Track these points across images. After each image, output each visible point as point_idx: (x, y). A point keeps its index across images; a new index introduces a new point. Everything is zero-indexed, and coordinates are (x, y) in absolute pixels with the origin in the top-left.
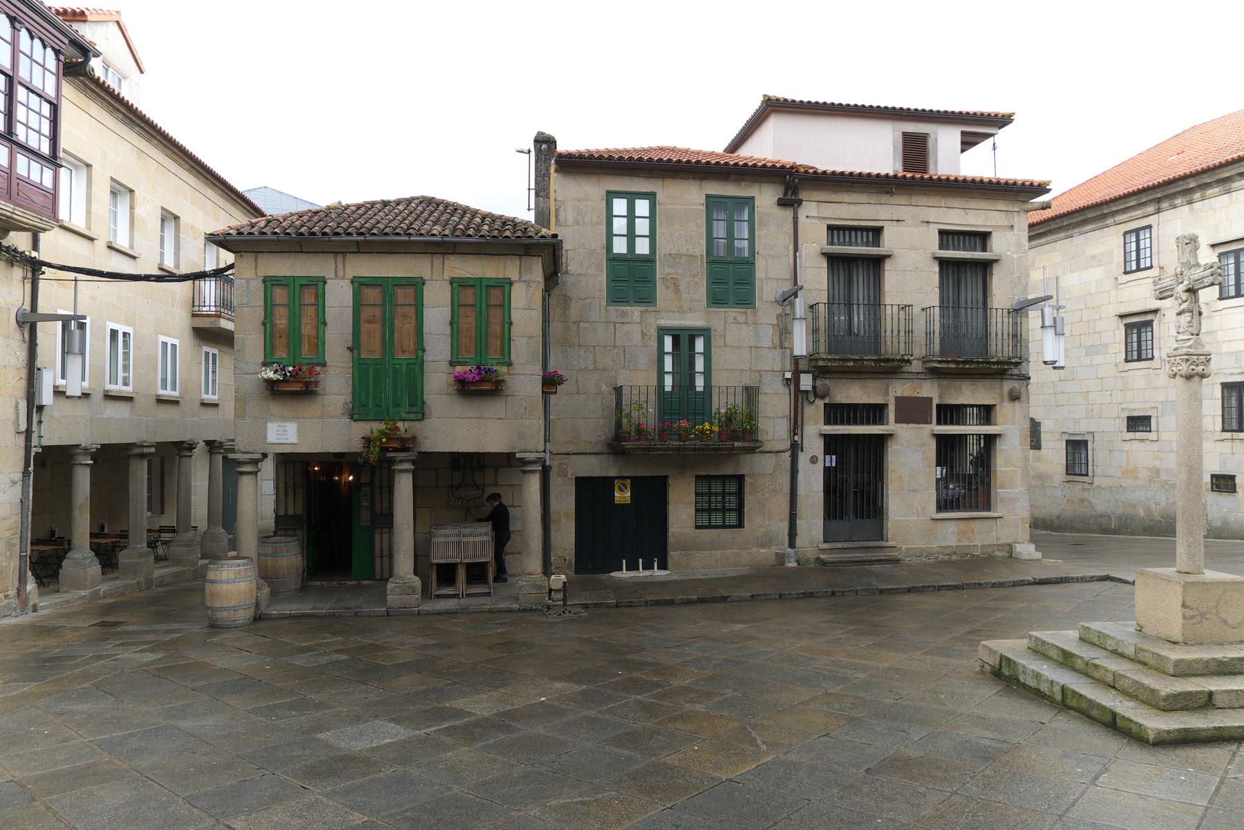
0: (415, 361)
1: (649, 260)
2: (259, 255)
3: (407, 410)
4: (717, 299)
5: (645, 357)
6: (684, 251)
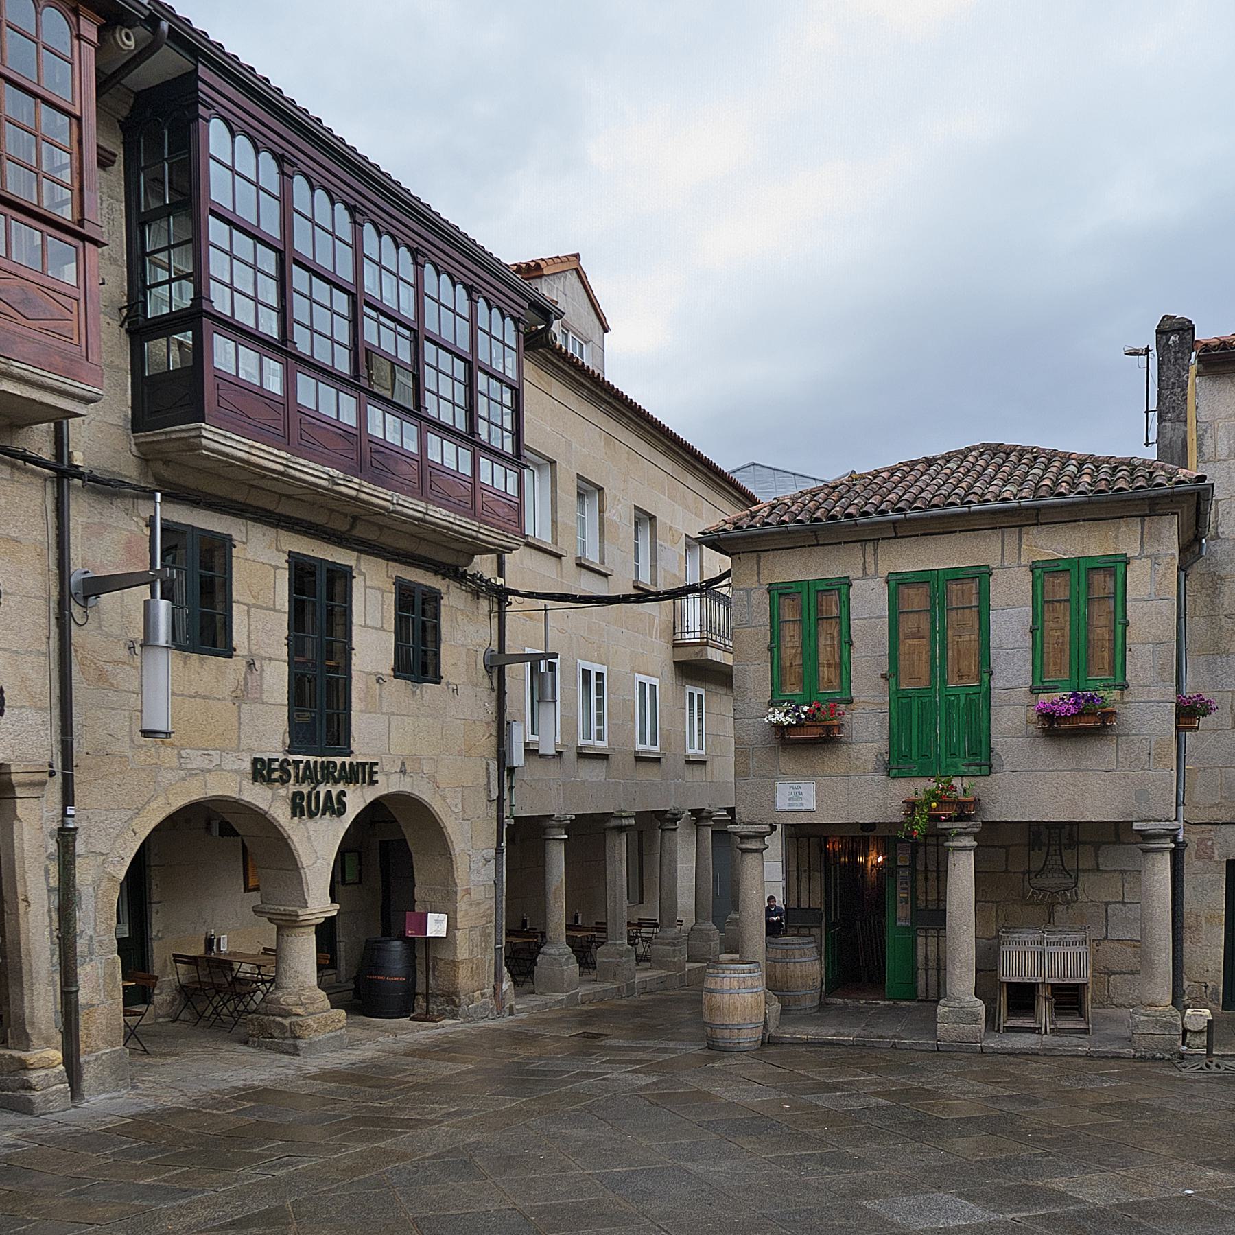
0: (976, 690)
2: (762, 555)
3: (966, 762)
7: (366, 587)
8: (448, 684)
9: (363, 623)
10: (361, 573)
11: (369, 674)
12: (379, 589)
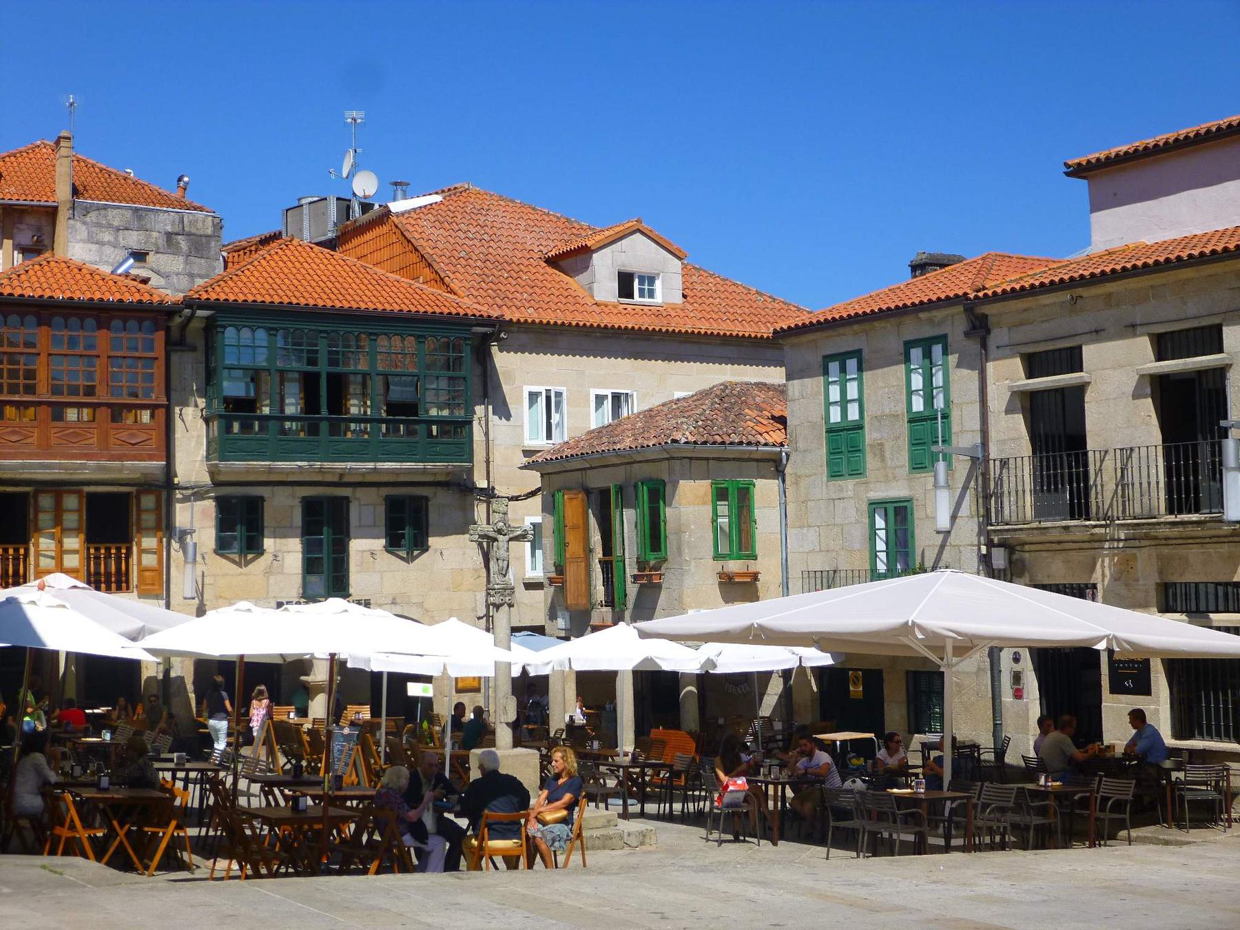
1: (858, 427)
4: (918, 465)
5: (858, 534)
6: (887, 411)
7: (360, 505)
8: (436, 550)
10: (356, 499)
11: (364, 551)
12: (371, 504)
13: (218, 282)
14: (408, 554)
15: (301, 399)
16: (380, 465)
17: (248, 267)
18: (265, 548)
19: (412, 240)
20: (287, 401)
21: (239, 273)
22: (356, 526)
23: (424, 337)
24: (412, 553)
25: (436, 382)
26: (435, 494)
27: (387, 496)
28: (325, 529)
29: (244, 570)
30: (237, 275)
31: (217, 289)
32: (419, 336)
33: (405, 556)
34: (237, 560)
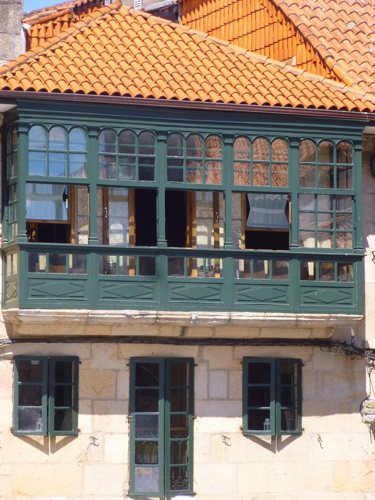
7: (209, 371)
9: (206, 397)
10: (202, 361)
11: (214, 434)
12: (224, 369)
13: (20, 65)
14: (273, 438)
15: (130, 224)
16: (236, 316)
17: (60, 44)
18: (79, 427)
19: (283, 7)
20: (112, 227)
21: (49, 53)
22: (204, 400)
23: (298, 140)
24: (279, 437)
25: (313, 202)
26: (311, 356)
27: (245, 358)
28: (161, 403)
29: (52, 457)
30: (45, 56)
31: (20, 75)
32: (291, 139)
33: (269, 441)
34: (42, 442)
